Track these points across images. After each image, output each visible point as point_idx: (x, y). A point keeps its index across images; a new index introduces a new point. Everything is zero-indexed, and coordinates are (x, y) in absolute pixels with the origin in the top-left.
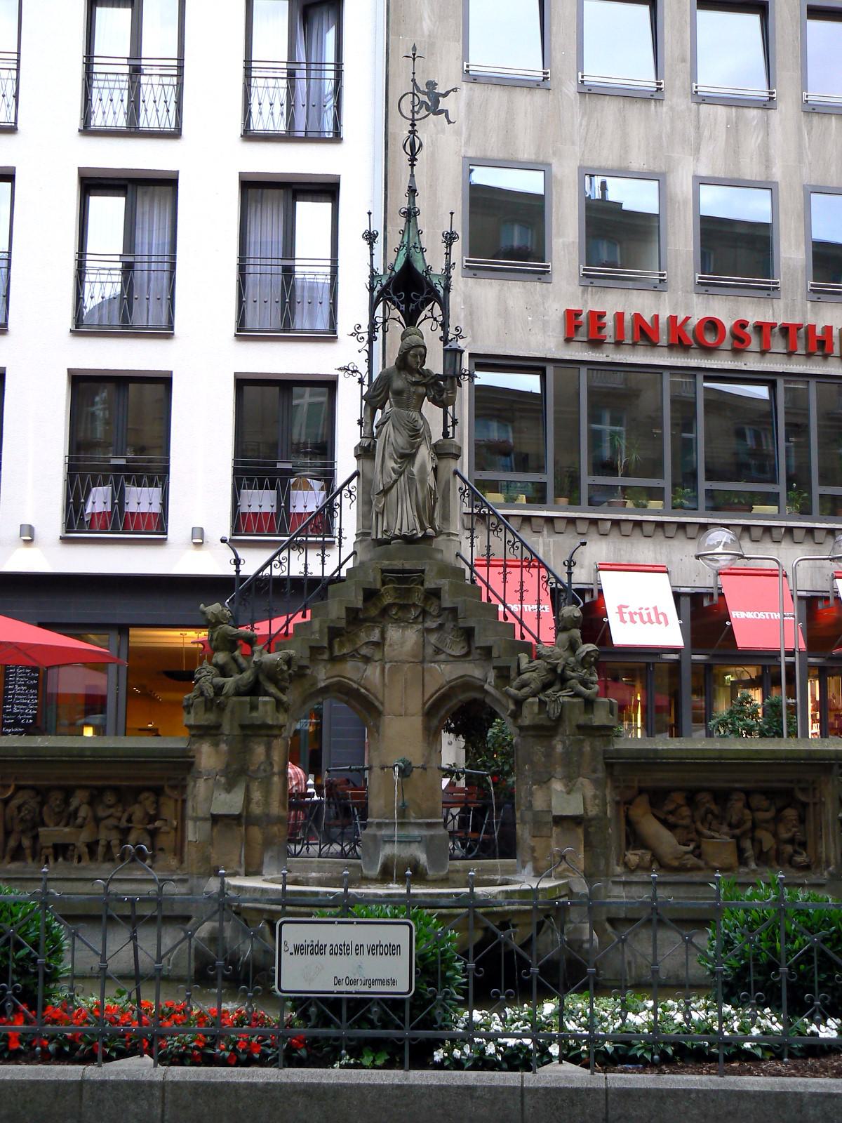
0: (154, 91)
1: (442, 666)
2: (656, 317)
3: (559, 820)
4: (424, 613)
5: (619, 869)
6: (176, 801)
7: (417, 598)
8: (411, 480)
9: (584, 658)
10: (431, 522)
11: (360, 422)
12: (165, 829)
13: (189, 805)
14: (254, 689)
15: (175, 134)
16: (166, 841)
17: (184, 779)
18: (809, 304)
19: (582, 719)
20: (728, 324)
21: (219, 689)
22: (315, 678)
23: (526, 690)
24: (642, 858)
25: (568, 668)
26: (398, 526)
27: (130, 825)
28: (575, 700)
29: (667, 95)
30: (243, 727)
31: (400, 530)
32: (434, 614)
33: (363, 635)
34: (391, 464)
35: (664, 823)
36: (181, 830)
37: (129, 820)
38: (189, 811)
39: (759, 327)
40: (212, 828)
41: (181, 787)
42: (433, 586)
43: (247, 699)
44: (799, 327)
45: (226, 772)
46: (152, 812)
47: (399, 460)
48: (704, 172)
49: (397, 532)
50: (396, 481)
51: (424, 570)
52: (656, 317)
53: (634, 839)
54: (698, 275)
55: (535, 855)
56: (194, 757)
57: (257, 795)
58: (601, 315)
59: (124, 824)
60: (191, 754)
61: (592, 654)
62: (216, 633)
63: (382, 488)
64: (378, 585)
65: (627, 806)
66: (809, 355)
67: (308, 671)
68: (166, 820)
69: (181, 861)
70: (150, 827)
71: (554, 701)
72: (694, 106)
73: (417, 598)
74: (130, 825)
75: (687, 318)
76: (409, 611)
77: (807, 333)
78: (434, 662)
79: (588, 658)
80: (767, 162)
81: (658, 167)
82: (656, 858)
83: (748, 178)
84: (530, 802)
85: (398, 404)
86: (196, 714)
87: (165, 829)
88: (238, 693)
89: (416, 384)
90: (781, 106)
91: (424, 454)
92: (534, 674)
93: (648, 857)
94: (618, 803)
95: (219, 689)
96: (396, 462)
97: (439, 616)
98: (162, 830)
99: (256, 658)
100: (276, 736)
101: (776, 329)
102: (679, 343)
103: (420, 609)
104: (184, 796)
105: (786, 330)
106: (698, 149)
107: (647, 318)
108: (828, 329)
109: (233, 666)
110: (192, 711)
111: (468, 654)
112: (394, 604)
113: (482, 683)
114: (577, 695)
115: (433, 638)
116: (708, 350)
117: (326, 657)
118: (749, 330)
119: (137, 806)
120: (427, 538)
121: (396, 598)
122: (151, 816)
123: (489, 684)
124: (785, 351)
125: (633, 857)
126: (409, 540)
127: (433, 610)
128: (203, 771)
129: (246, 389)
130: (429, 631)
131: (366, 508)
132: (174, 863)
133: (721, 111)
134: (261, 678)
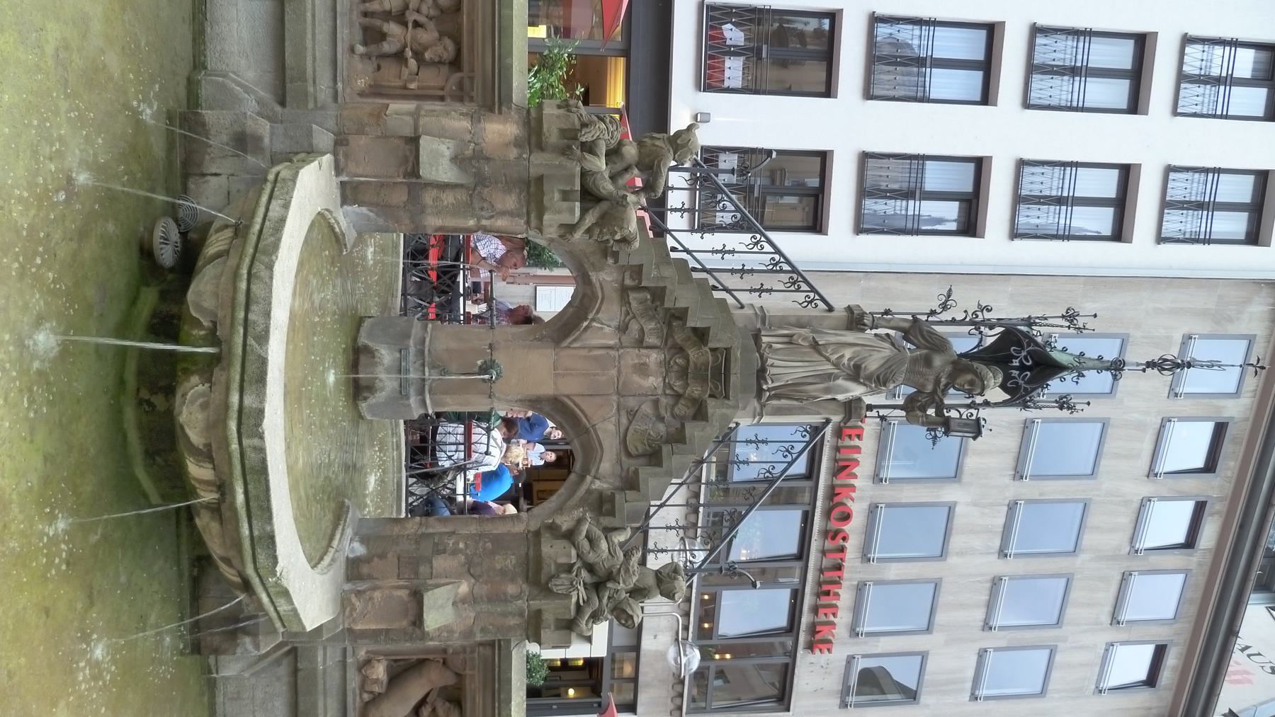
0: (1060, 89)
1: (613, 419)
2: (855, 476)
3: (417, 597)
4: (678, 397)
5: (362, 654)
6: (442, 89)
7: (695, 390)
8: (829, 377)
9: (625, 611)
10: (778, 397)
11: (887, 312)
12: (406, 72)
13: (437, 106)
14: (589, 196)
15: (1027, 104)
16: (390, 73)
17: (471, 99)
18: (856, 583)
19: (548, 617)
20: (847, 528)
21: (589, 148)
22: (601, 269)
23: (586, 544)
24: (376, 681)
26: (777, 363)
27: (410, 25)
28: (573, 607)
30: (540, 179)
31: (772, 366)
33: (652, 325)
34: (848, 353)
35: (422, 702)
36: (404, 94)
37: (417, 24)
38: (428, 106)
39: (842, 550)
40: (401, 137)
41: (461, 95)
42: (710, 411)
43: (578, 187)
45: (480, 156)
46: (427, 55)
47: (852, 363)
48: (958, 509)
49: (770, 362)
50: (828, 359)
52: (855, 476)
53: (401, 672)
55: (376, 559)
56: (500, 113)
57: (449, 198)
58: (859, 437)
59: (411, 16)
60: (504, 109)
62: (663, 145)
63: (820, 343)
64: (711, 345)
65: (442, 661)
67: (610, 261)
68: (417, 74)
69: (362, 94)
70: (409, 53)
71: (572, 584)
72: (1007, 502)
73: (695, 390)
74: (410, 25)
75: (852, 499)
76: (677, 379)
78: (618, 409)
79: (624, 616)
80: (961, 554)
81: (966, 478)
82: (376, 699)
83: (952, 540)
84: (444, 552)
85: (914, 361)
86: (558, 117)
87: (406, 72)
88: (584, 174)
89: (937, 382)
90: (1001, 562)
91: (857, 390)
92: (605, 554)
93: (377, 689)
94: (445, 651)
95: (589, 148)
96: (850, 359)
97: (673, 416)
98: (404, 68)
99: (631, 198)
100: (528, 223)
102: (832, 493)
103: (681, 391)
104: (449, 100)
105: (839, 568)
106: (975, 504)
107: (856, 470)
108: (837, 595)
109: (619, 166)
110: (562, 111)
112: (688, 360)
113: (593, 473)
115: (647, 408)
116: (828, 514)
117: (628, 282)
119: (436, 35)
120: (760, 392)
121: (695, 364)
122: (423, 54)
123: (592, 482)
124: (823, 567)
125: (380, 671)
126: (761, 373)
127: (681, 409)
128: (482, 125)
129: (818, 159)
130: (656, 403)
131: (793, 320)
132: (361, 83)
133: (1001, 521)
134: (604, 206)
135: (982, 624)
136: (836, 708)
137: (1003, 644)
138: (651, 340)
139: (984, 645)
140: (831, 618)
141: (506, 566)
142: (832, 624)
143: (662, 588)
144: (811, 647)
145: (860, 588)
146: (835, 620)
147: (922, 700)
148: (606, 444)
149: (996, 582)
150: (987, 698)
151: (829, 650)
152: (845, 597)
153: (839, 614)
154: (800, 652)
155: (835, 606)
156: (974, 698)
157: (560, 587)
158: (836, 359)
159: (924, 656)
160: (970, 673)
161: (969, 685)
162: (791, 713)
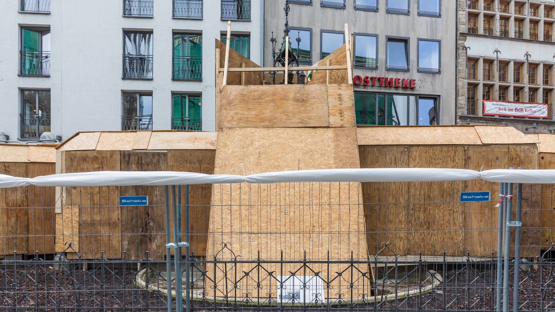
18: (386, 72)
20: (363, 78)
29: (346, 8)
39: (372, 78)
44: (383, 78)
54: (354, 63)
66: (386, 87)
72: (355, 11)
77: (385, 80)
90: (380, 11)
101: (377, 79)
105: (379, 79)
108: (392, 79)
118: (369, 79)
133: (362, 12)
135: (406, 16)
136: (441, 75)
137: (416, 6)
139: (416, 14)
140: (400, 81)
142: (403, 80)
144: (412, 89)
145: (389, 70)
146: (401, 79)
147: (439, 39)
149: (389, 12)
150: (440, 10)
151: (414, 81)
152: (392, 76)
153: (399, 77)
154: (415, 92)
155: (395, 79)
156: (440, 16)
159: (420, 40)
160: (428, 19)
161: (434, 19)
162: (441, 94)
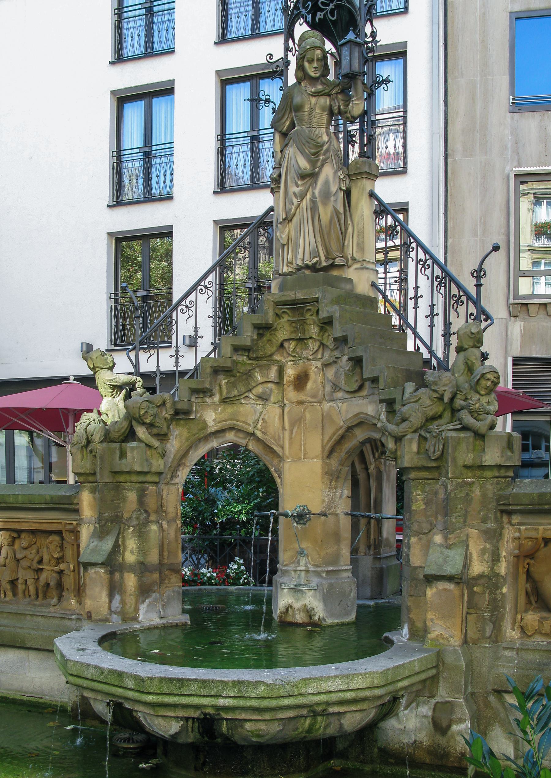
25: (459, 396)
26: (300, 255)
28: (462, 435)
32: (331, 347)
47: (300, 183)
49: (299, 263)
51: (318, 298)
61: (489, 376)
63: (284, 217)
73: (314, 330)
78: (333, 401)
96: (297, 186)
111: (360, 388)
114: (465, 428)
138: (273, 374)
141: (423, 500)
143: (467, 347)
148: (356, 410)
157: (437, 449)
158: (297, 198)
